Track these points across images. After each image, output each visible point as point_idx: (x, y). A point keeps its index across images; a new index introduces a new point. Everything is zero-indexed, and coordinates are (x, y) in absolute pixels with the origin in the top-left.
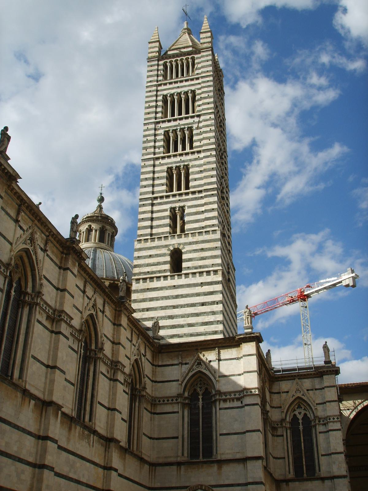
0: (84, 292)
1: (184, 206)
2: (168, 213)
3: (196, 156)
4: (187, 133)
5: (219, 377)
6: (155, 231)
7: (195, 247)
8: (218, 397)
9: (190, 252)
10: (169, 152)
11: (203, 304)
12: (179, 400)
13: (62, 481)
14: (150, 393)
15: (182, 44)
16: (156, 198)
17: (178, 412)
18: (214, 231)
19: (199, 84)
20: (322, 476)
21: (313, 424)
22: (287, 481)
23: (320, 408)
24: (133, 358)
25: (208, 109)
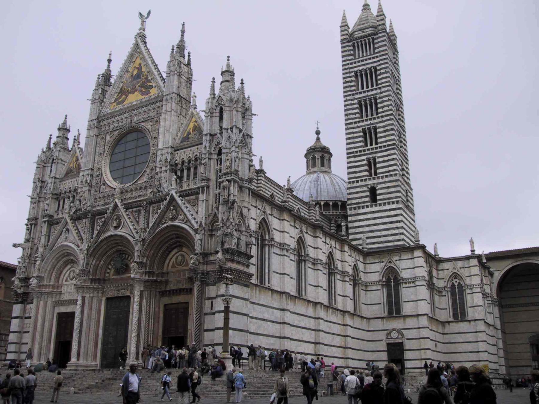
0: (325, 243)
1: (375, 156)
2: (365, 162)
3: (380, 120)
4: (373, 101)
5: (402, 269)
6: (358, 175)
7: (384, 185)
8: (401, 281)
9: (381, 189)
10: (363, 118)
11: (391, 223)
12: (380, 283)
13: (327, 334)
14: (364, 280)
15: (364, 24)
16: (357, 152)
17: (380, 290)
18: (395, 175)
19: (379, 61)
20: (469, 319)
21: (464, 289)
22: (449, 322)
23: (468, 279)
24: (353, 265)
25: (386, 82)
